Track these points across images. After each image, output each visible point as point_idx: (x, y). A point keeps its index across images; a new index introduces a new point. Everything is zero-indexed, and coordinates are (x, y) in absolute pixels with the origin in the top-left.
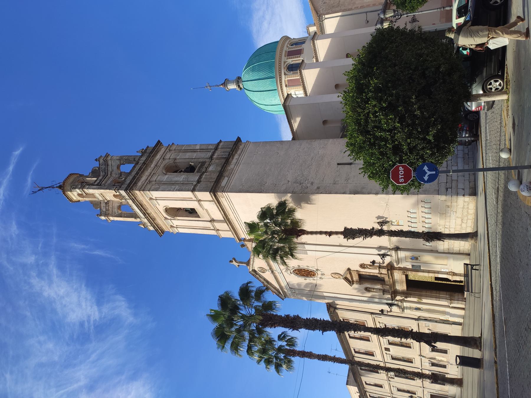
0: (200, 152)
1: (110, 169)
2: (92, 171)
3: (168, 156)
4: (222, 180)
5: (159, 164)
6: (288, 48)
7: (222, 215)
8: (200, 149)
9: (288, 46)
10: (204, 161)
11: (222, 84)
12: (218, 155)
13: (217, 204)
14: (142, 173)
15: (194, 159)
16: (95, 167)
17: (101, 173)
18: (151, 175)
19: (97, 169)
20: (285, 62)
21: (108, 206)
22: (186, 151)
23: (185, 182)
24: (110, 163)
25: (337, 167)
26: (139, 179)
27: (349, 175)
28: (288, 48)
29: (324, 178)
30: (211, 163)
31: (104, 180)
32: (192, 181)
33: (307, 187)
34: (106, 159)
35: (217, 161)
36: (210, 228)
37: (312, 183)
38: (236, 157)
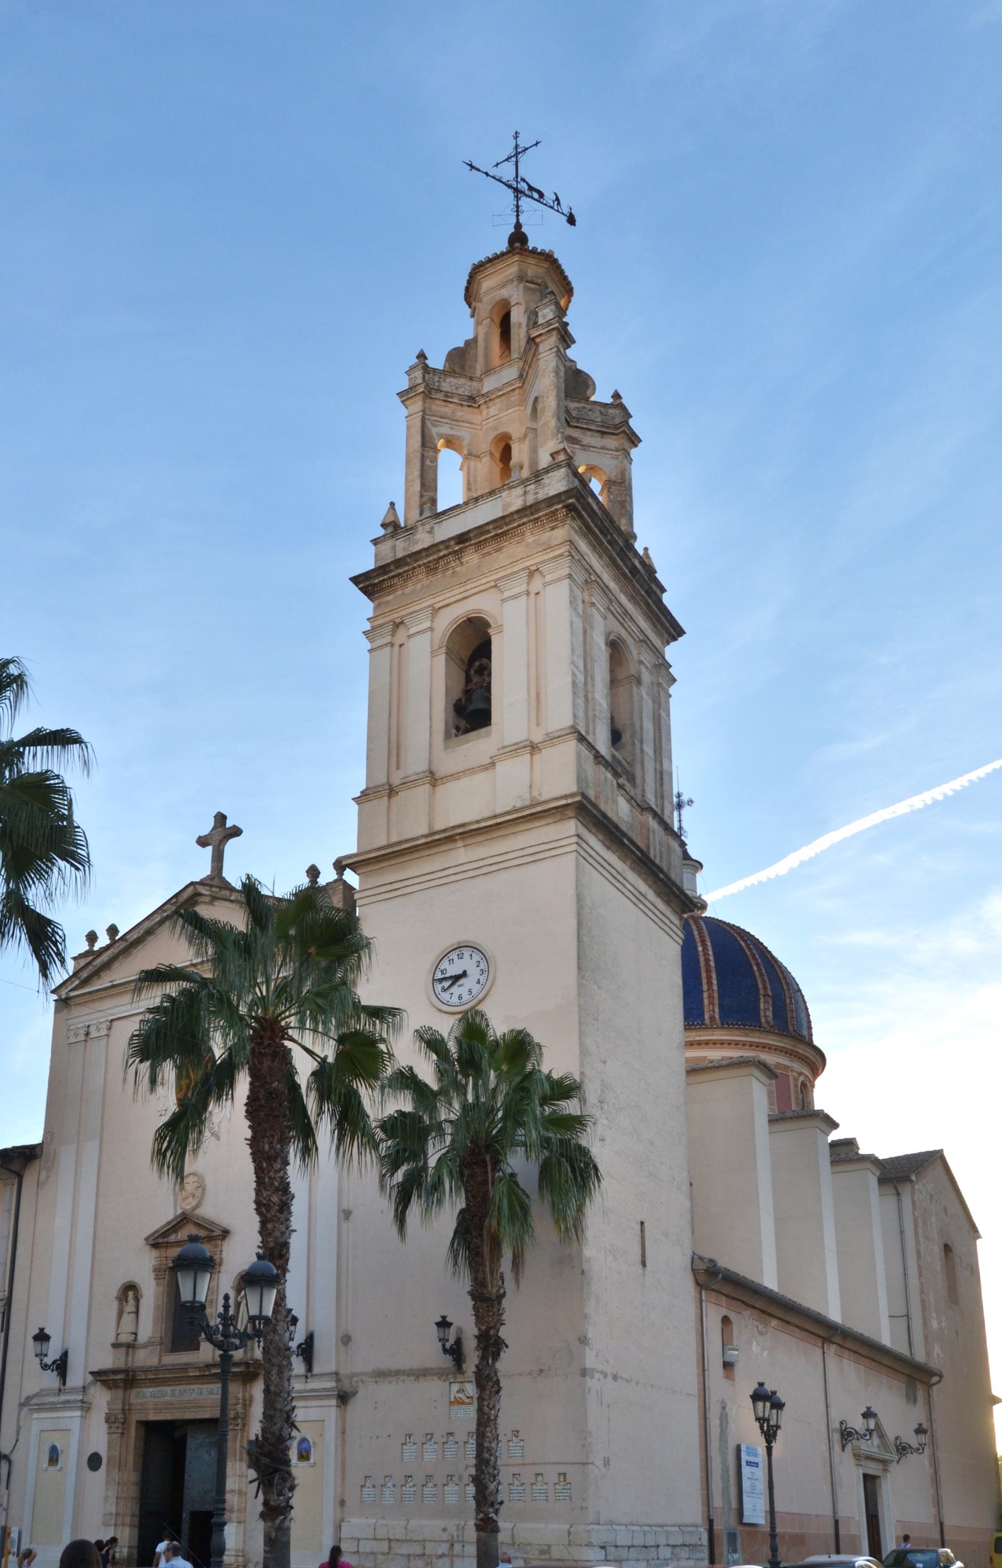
4: (601, 837)
5: (630, 624)
7: (478, 822)
12: (654, 832)
16: (594, 389)
18: (605, 589)
21: (462, 405)
34: (624, 431)
36: (398, 768)
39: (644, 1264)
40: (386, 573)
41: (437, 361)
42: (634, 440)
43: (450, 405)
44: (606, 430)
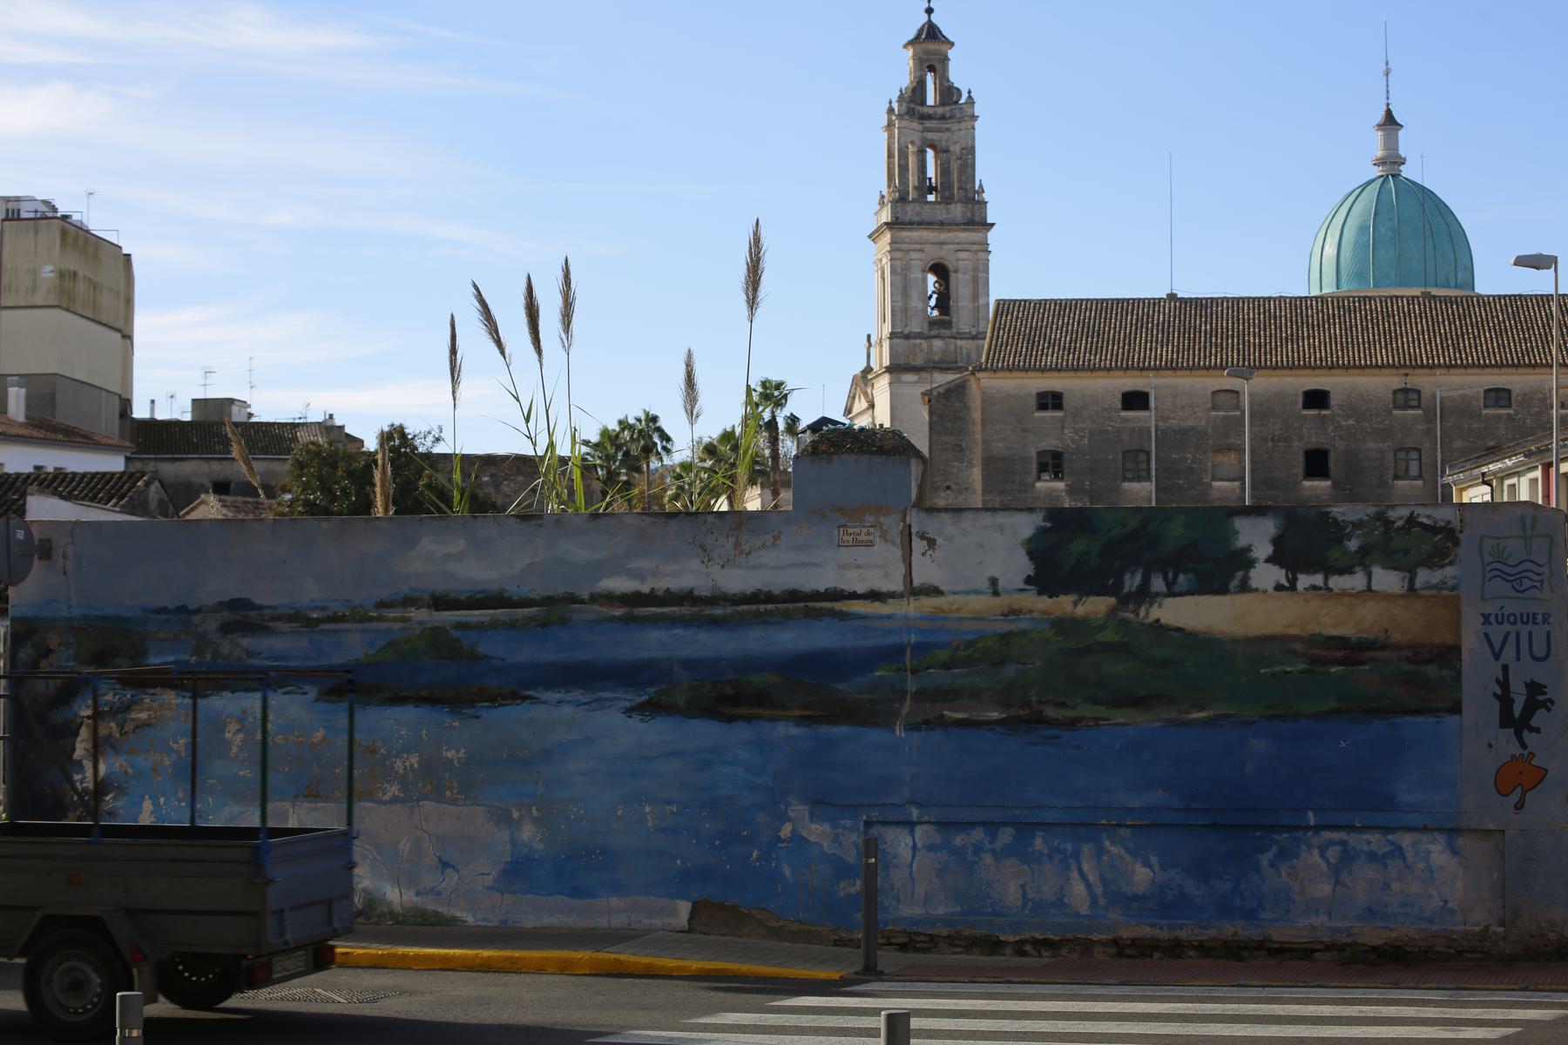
0: (974, 307)
1: (955, 127)
8: (978, 307)
10: (953, 325)
11: (1389, 113)
12: (961, 348)
15: (958, 306)
17: (948, 108)
19: (955, 99)
22: (975, 281)
23: (909, 314)
24: (963, 125)
26: (911, 230)
35: (952, 347)
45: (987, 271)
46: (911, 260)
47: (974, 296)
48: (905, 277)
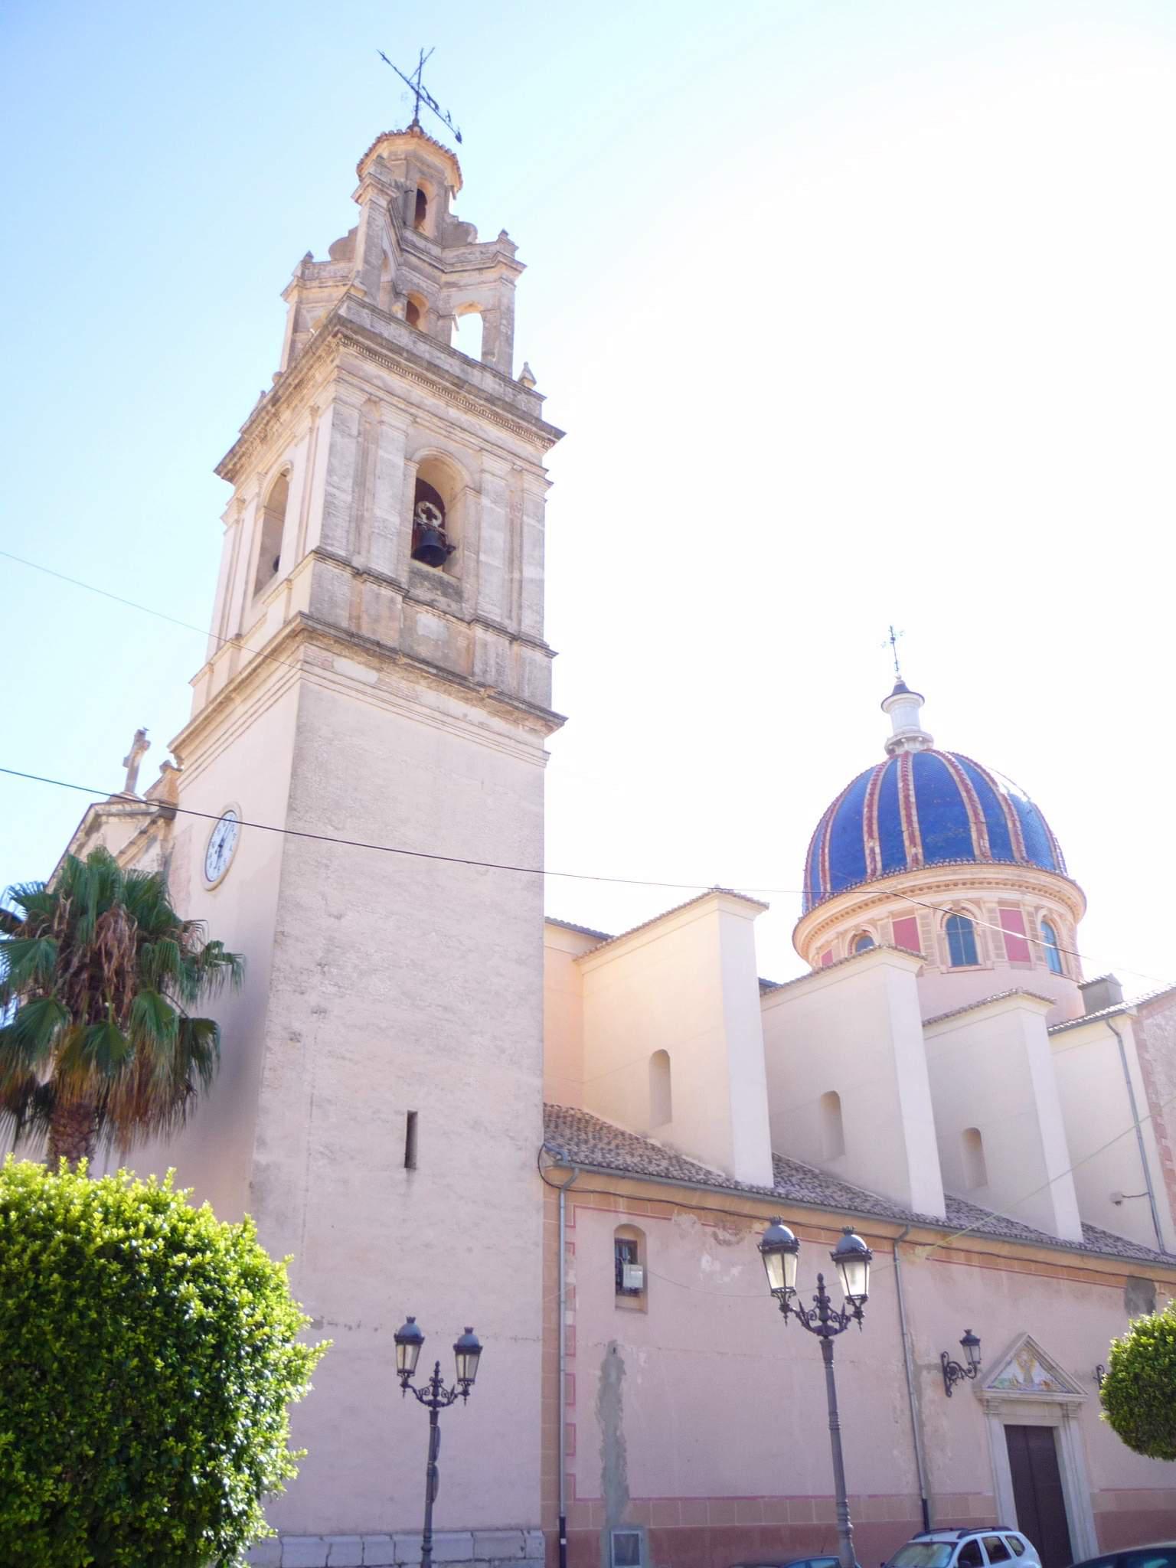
2: (463, 223)
3: (490, 463)
6: (1032, 909)
8: (521, 582)
9: (1043, 912)
13: (269, 649)
14: (419, 376)
15: (478, 561)
20: (977, 903)
21: (337, 286)
22: (515, 530)
23: (365, 527)
24: (491, 275)
25: (397, 1113)
27: (352, 1158)
28: (1032, 909)
29: (343, 1058)
30: (454, 620)
31: (424, 261)
32: (369, 551)
33: (302, 993)
34: (499, 262)
35: (462, 643)
37: (319, 1011)
38: (477, 713)
39: (409, 1162)
40: (235, 455)
41: (322, 255)
42: (517, 267)
43: (325, 290)
44: (482, 266)
45: (541, 519)
46: (381, 422)
47: (511, 561)
48: (364, 454)
